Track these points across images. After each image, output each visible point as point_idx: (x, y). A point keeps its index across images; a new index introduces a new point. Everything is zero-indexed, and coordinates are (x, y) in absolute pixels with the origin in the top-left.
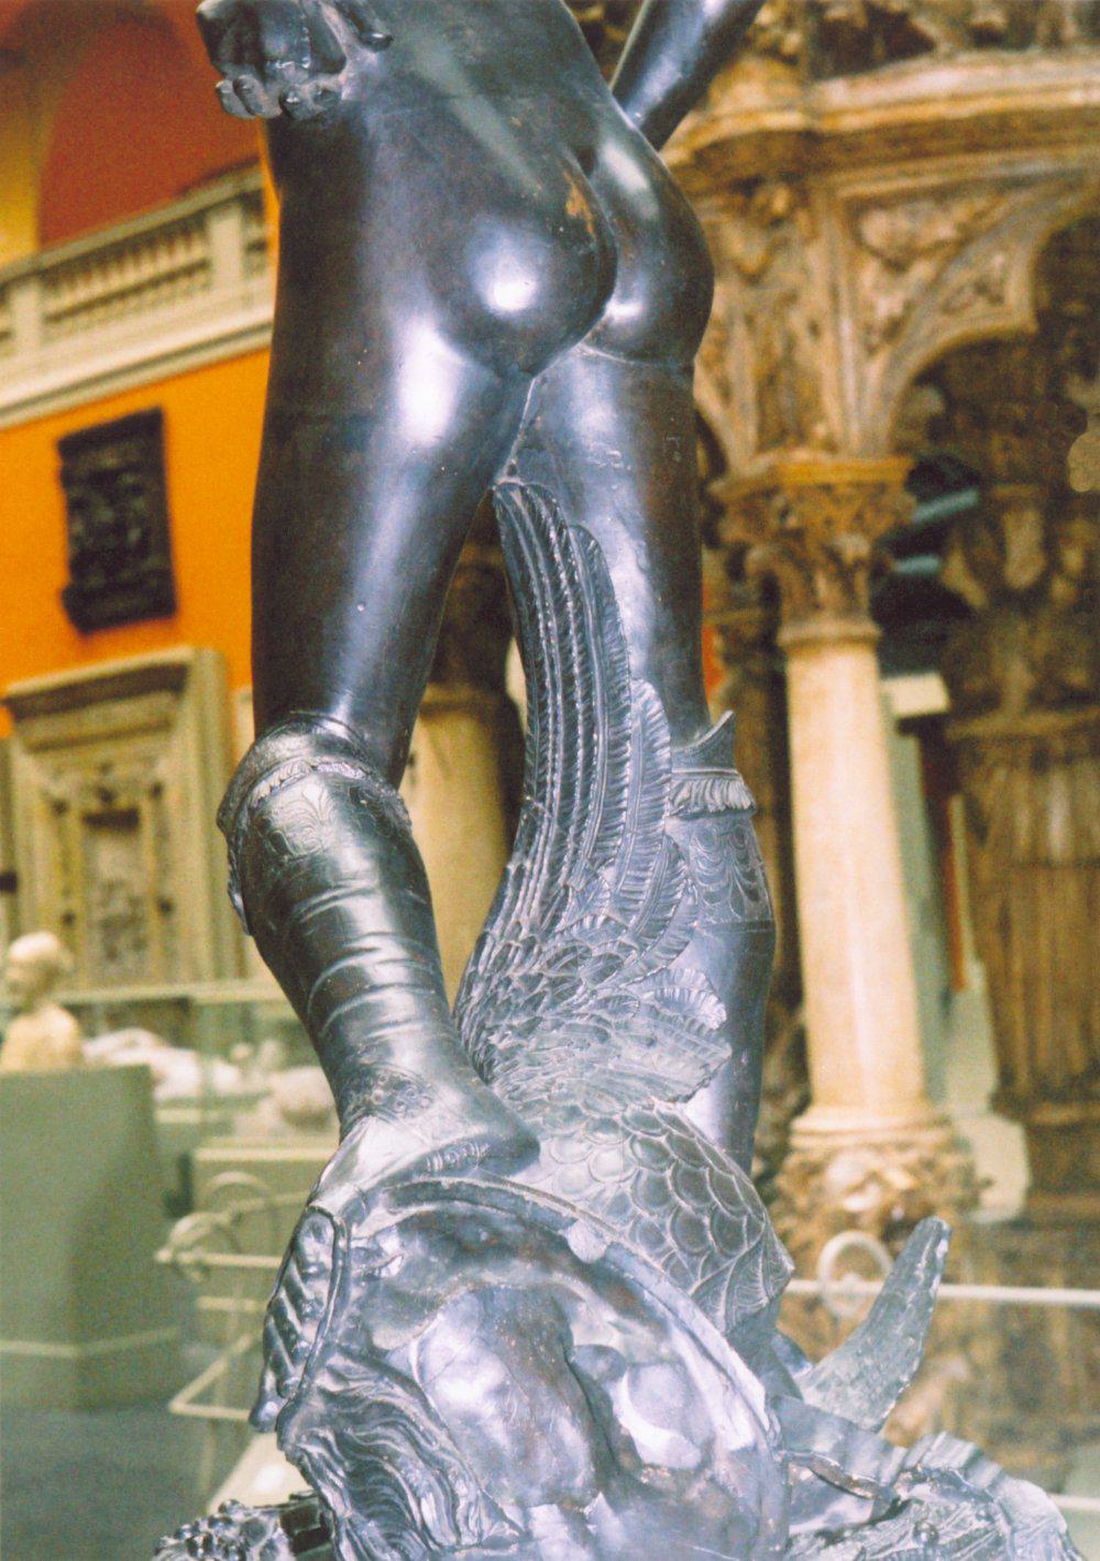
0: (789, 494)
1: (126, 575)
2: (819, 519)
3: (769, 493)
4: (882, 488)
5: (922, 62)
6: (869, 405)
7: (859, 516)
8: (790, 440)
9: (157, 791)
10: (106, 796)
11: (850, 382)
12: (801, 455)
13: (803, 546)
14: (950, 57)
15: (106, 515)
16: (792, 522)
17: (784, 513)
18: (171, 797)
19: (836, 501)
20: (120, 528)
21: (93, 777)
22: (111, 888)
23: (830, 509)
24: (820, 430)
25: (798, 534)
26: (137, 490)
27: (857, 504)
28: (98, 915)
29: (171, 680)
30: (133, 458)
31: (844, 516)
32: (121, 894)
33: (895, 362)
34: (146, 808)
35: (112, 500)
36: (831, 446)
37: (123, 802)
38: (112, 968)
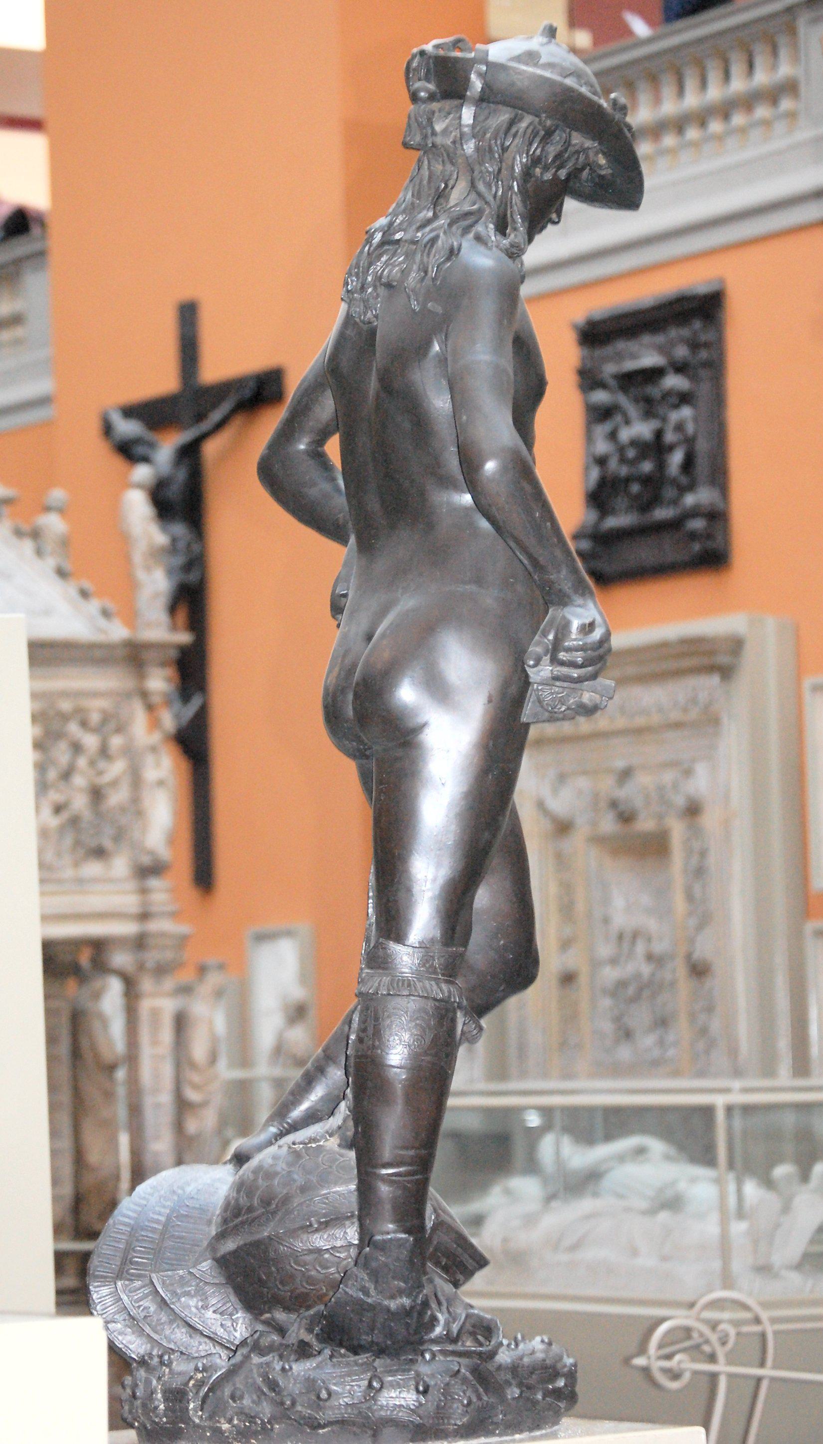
1: (662, 513)
9: (693, 810)
10: (626, 817)
15: (642, 429)
18: (710, 820)
20: (657, 448)
21: (607, 785)
22: (627, 939)
26: (684, 398)
28: (610, 974)
29: (716, 660)
30: (681, 352)
32: (640, 948)
34: (677, 830)
35: (650, 408)
37: (645, 824)
38: (625, 1053)
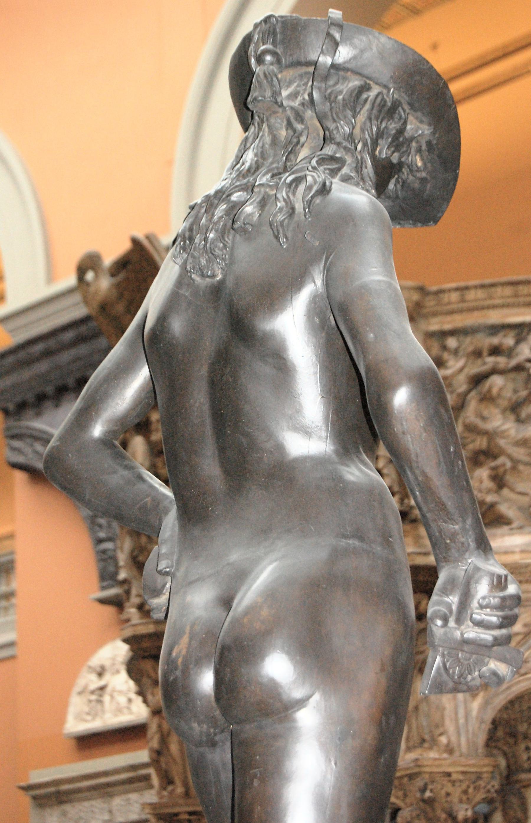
0: (427, 776)
2: (443, 793)
3: (411, 777)
4: (479, 776)
5: (505, 529)
6: (473, 725)
7: (465, 792)
8: (426, 745)
11: (461, 712)
12: (433, 754)
13: (433, 810)
14: (521, 528)
16: (428, 794)
17: (423, 790)
19: (453, 783)
23: (449, 788)
24: (443, 740)
25: (430, 802)
27: (464, 786)
31: (456, 793)
33: (486, 703)
36: (449, 750)
